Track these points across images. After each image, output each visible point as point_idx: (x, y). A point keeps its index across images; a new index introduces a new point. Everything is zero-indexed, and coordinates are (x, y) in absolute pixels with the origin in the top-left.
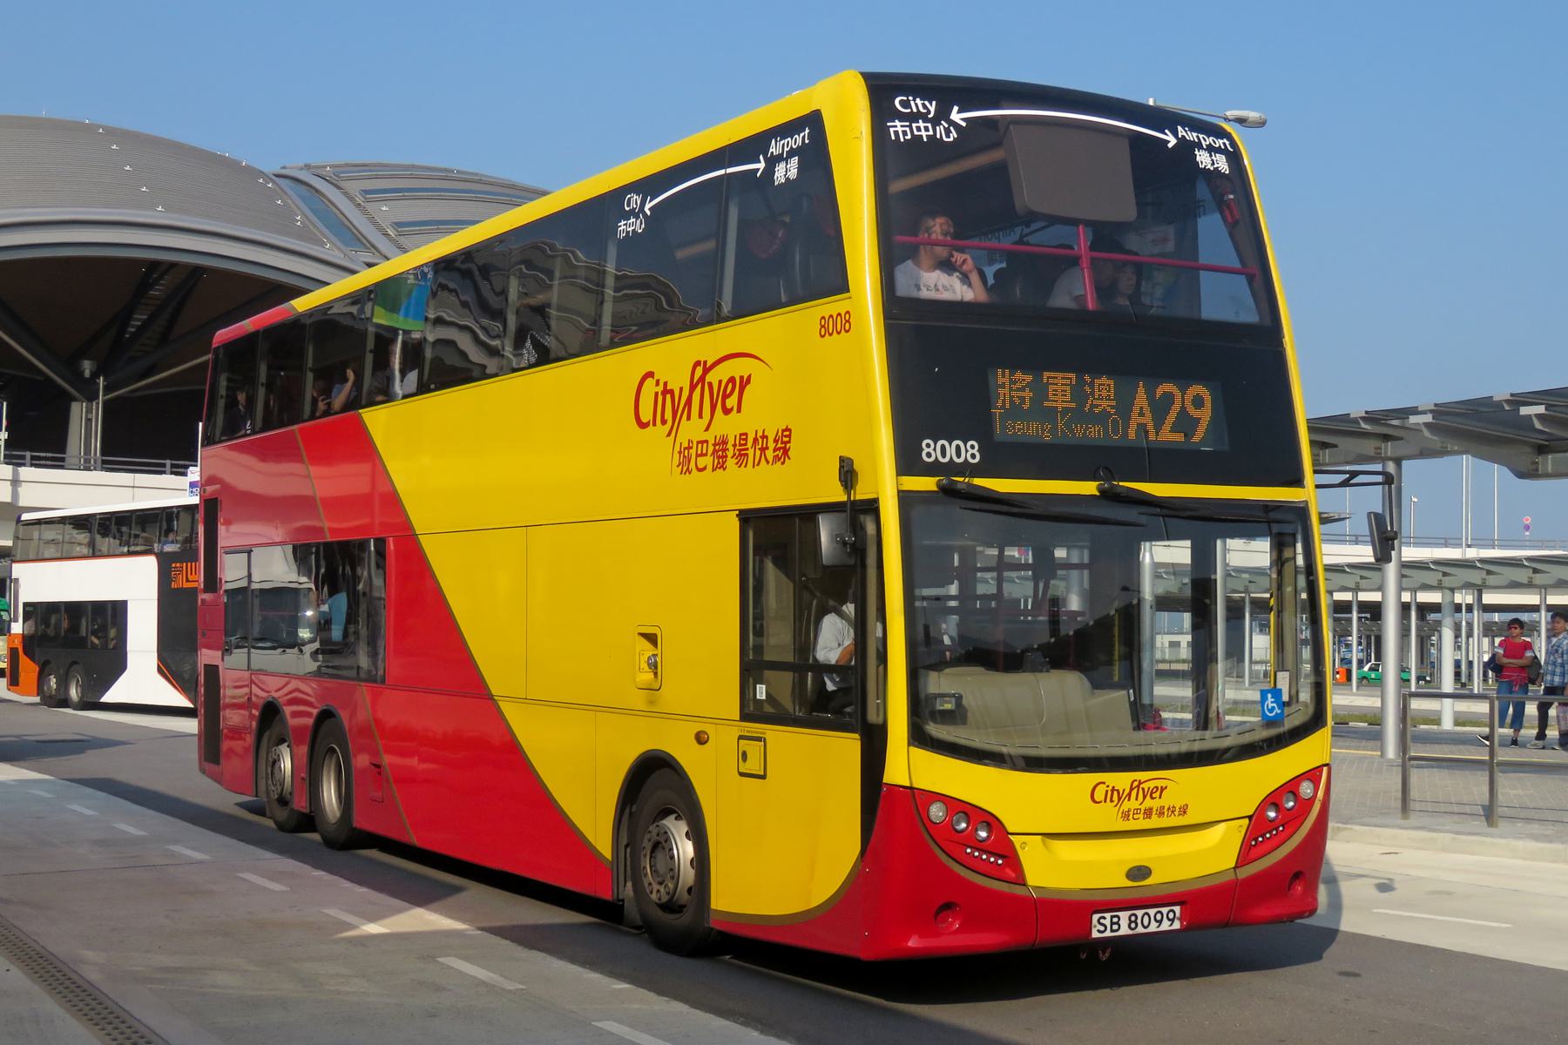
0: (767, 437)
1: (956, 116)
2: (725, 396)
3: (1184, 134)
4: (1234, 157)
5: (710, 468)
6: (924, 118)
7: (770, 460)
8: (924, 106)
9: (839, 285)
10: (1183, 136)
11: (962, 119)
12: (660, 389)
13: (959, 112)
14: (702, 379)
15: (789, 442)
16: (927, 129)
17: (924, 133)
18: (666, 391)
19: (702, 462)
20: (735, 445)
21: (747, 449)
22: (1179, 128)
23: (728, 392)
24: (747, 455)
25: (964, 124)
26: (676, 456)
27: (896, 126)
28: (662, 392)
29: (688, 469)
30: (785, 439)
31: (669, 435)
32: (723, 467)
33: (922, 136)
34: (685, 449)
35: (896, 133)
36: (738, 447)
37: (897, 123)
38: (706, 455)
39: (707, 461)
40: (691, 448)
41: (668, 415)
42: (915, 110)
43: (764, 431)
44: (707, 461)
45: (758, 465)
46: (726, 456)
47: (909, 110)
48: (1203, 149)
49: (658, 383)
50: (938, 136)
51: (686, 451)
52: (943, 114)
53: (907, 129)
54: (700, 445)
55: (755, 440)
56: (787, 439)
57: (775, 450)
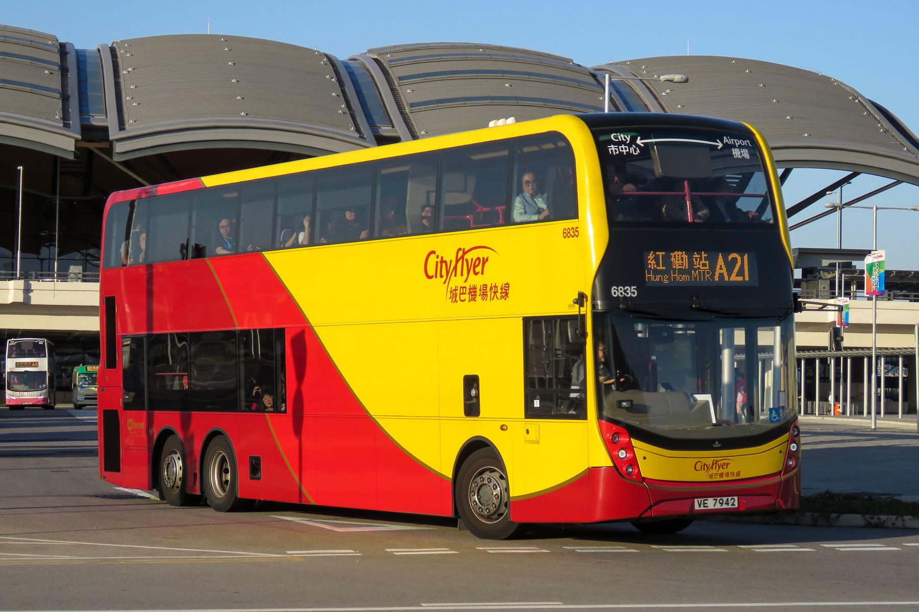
0: (497, 287)
2: (475, 267)
5: (467, 300)
7: (499, 297)
12: (439, 260)
14: (462, 257)
15: (508, 290)
18: (442, 261)
19: (463, 297)
20: (480, 290)
21: (487, 292)
23: (477, 264)
24: (487, 295)
26: (449, 294)
28: (440, 262)
29: (455, 300)
30: (507, 288)
31: (445, 283)
32: (474, 300)
34: (453, 290)
36: (482, 291)
38: (465, 294)
39: (466, 297)
40: (457, 290)
41: (444, 273)
43: (495, 284)
44: (466, 297)
45: (493, 299)
46: (476, 295)
49: (438, 257)
51: (454, 293)
54: (462, 289)
55: (491, 288)
56: (507, 288)
57: (501, 293)
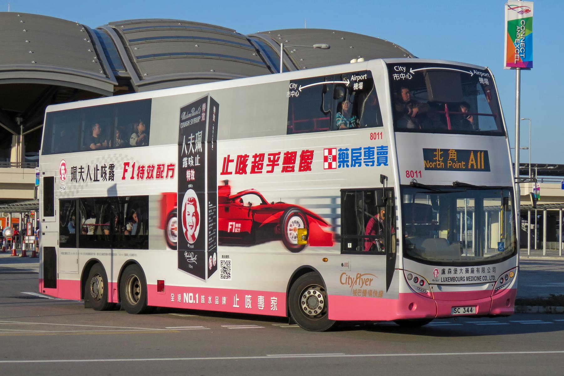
1: (411, 71)
3: (476, 72)
4: (490, 79)
6: (402, 72)
8: (402, 68)
9: (381, 124)
10: (475, 73)
11: (414, 72)
13: (412, 70)
16: (404, 76)
17: (403, 77)
22: (474, 71)
25: (414, 73)
27: (395, 76)
33: (403, 78)
35: (395, 78)
37: (396, 75)
42: (400, 70)
47: (398, 70)
48: (481, 77)
50: (407, 78)
52: (408, 71)
53: (398, 76)
